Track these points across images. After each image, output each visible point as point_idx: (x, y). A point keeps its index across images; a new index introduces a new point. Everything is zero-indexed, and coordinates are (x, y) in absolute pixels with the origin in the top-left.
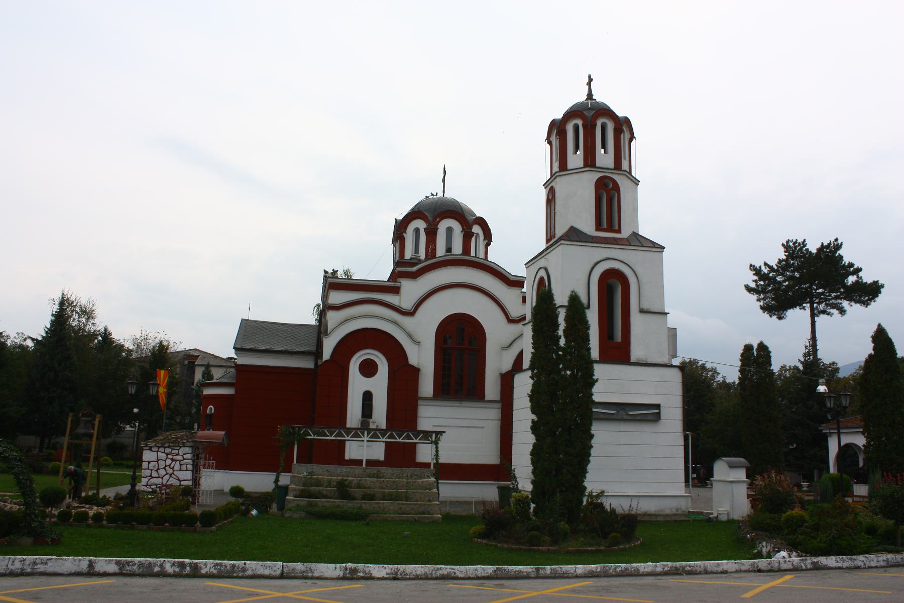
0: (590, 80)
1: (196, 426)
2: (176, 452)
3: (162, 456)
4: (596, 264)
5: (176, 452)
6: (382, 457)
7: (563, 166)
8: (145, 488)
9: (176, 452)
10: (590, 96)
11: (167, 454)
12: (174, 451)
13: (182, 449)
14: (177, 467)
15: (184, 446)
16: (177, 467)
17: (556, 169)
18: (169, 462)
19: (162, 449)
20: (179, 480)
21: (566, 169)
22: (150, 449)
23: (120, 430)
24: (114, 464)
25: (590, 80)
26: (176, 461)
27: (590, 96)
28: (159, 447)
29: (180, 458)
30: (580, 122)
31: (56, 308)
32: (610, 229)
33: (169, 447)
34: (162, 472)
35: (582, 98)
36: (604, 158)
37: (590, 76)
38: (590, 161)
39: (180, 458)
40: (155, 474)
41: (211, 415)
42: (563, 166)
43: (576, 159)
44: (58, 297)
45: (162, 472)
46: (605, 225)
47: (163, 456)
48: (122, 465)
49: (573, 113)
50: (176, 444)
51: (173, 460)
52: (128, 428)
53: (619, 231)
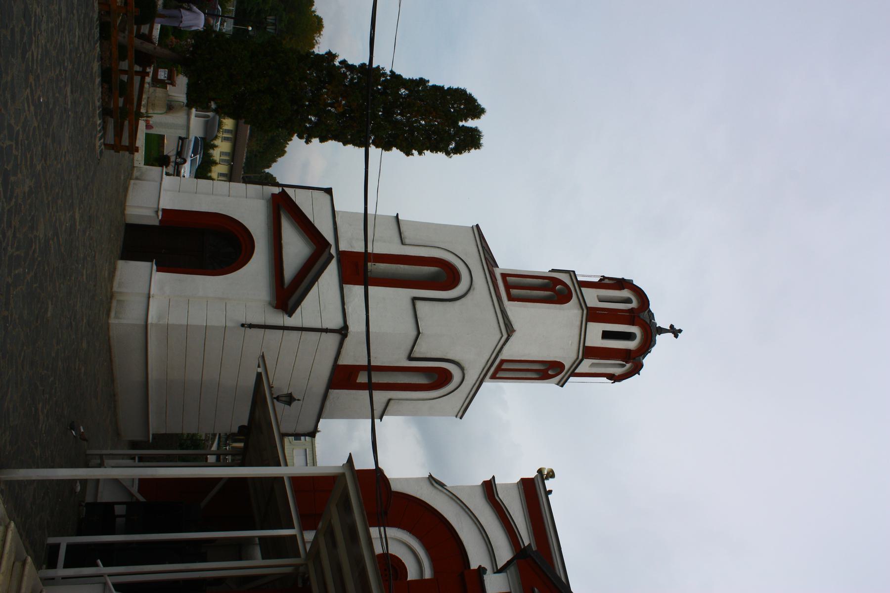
0: (676, 332)
4: (462, 369)
7: (593, 315)
10: (661, 331)
17: (592, 297)
21: (588, 320)
25: (676, 332)
27: (661, 331)
30: (634, 304)
32: (499, 369)
35: (661, 321)
36: (586, 366)
37: (680, 331)
38: (590, 352)
46: (504, 366)
53: (494, 377)
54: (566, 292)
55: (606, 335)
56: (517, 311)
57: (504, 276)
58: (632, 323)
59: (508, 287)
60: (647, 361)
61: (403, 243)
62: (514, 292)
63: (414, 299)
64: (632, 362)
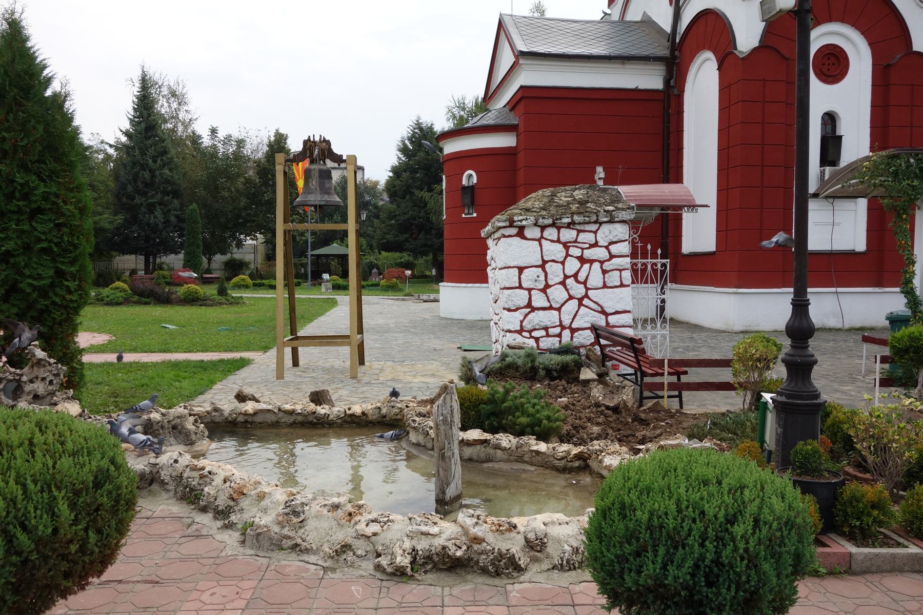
1: (600, 172)
2: (588, 238)
3: (554, 251)
5: (590, 238)
6: (859, 244)
8: (519, 339)
9: (588, 238)
11: (566, 246)
12: (583, 237)
13: (605, 228)
14: (596, 278)
15: (611, 222)
16: (596, 278)
18: (572, 265)
19: (551, 233)
20: (603, 312)
22: (521, 234)
23: (240, 244)
24: (255, 285)
26: (591, 262)
28: (543, 228)
29: (600, 253)
31: (136, 89)
33: (568, 226)
34: (558, 294)
39: (600, 253)
40: (539, 300)
41: (471, 189)
44: (137, 76)
45: (558, 294)
47: (557, 251)
48: (263, 285)
50: (587, 216)
51: (582, 260)
52: (249, 242)
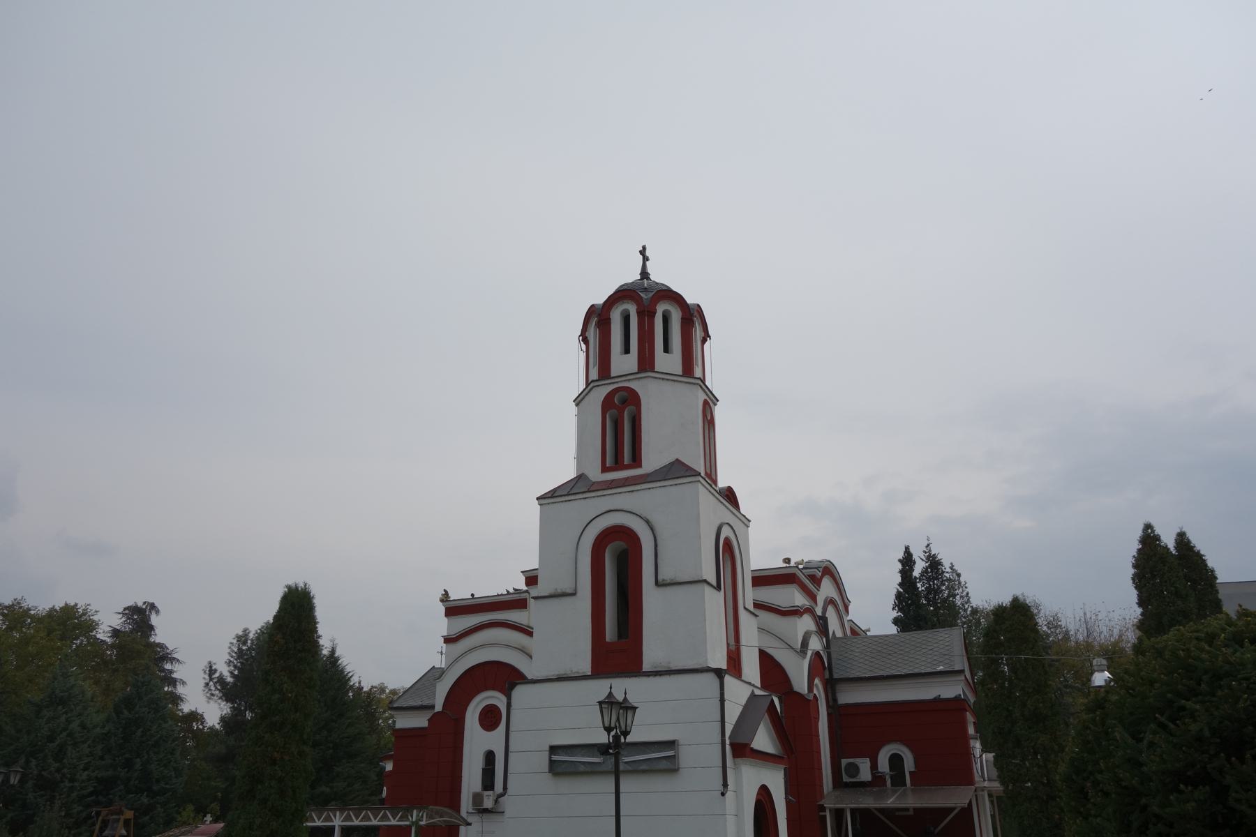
10: (645, 274)
17: (624, 363)
27: (645, 274)
35: (635, 276)
36: (698, 373)
42: (646, 363)
43: (669, 362)
49: (623, 294)
54: (624, 394)
55: (666, 349)
56: (652, 459)
57: (605, 469)
58: (652, 314)
59: (618, 465)
60: (690, 300)
61: (574, 594)
62: (626, 461)
63: (657, 583)
64: (692, 317)
